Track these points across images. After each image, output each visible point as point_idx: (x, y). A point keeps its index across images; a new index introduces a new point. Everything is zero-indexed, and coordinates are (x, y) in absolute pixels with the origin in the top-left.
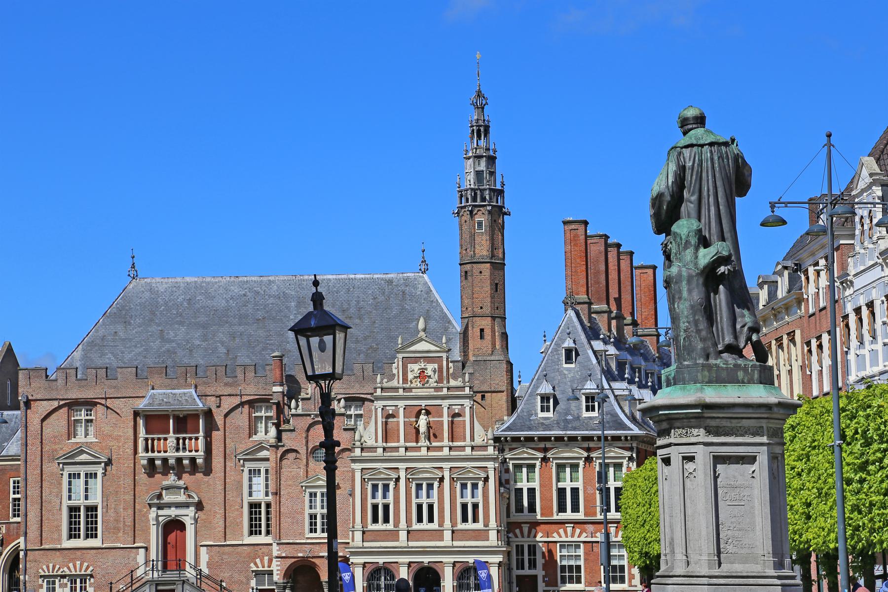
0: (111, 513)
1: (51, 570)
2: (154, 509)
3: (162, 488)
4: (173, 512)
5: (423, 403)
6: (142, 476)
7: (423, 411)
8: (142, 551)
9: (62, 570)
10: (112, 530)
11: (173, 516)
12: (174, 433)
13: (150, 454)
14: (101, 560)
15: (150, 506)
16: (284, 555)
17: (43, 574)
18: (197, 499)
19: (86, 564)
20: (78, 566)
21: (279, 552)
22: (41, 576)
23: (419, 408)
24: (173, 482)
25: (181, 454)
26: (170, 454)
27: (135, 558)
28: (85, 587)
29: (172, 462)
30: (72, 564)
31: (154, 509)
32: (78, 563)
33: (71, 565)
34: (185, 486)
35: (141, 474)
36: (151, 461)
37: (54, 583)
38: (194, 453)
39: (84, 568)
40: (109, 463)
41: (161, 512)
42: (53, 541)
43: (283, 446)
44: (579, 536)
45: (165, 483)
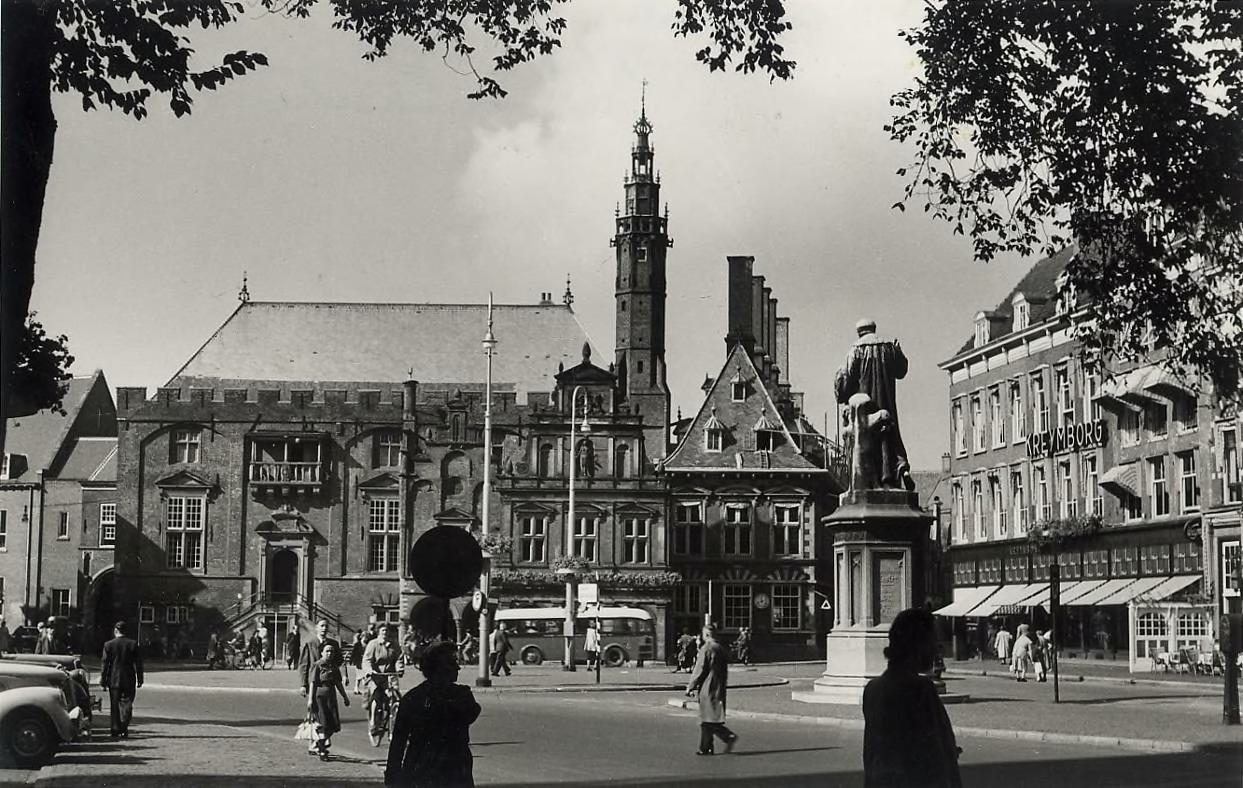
4: (285, 543)
12: (289, 460)
16: (412, 591)
41: (272, 543)
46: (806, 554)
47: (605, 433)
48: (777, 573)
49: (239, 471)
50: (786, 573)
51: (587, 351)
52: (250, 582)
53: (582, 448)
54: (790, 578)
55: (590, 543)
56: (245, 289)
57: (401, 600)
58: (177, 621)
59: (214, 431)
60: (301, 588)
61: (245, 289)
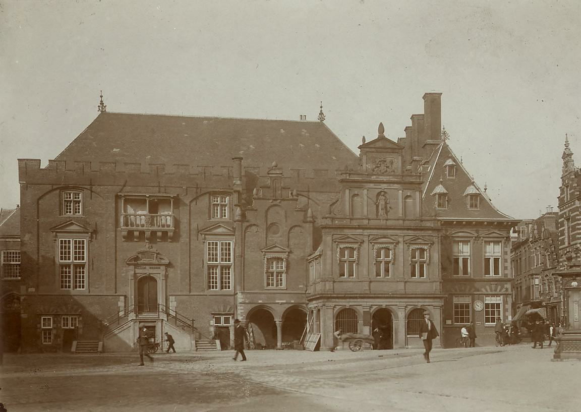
4: (148, 271)
5: (384, 186)
7: (383, 193)
8: (122, 298)
13: (130, 227)
16: (247, 302)
18: (167, 262)
21: (243, 300)
23: (380, 190)
24: (148, 249)
25: (155, 228)
26: (147, 228)
29: (148, 234)
31: (132, 267)
34: (157, 252)
36: (131, 233)
38: (166, 228)
40: (95, 232)
41: (138, 271)
43: (248, 221)
44: (469, 291)
45: (142, 250)
46: (506, 275)
47: (396, 186)
48: (488, 287)
49: (112, 221)
50: (493, 286)
51: (381, 128)
52: (123, 297)
53: (381, 197)
54: (496, 291)
55: (387, 263)
56: (102, 103)
57: (238, 308)
58: (70, 327)
59: (92, 191)
60: (161, 300)
61: (102, 103)
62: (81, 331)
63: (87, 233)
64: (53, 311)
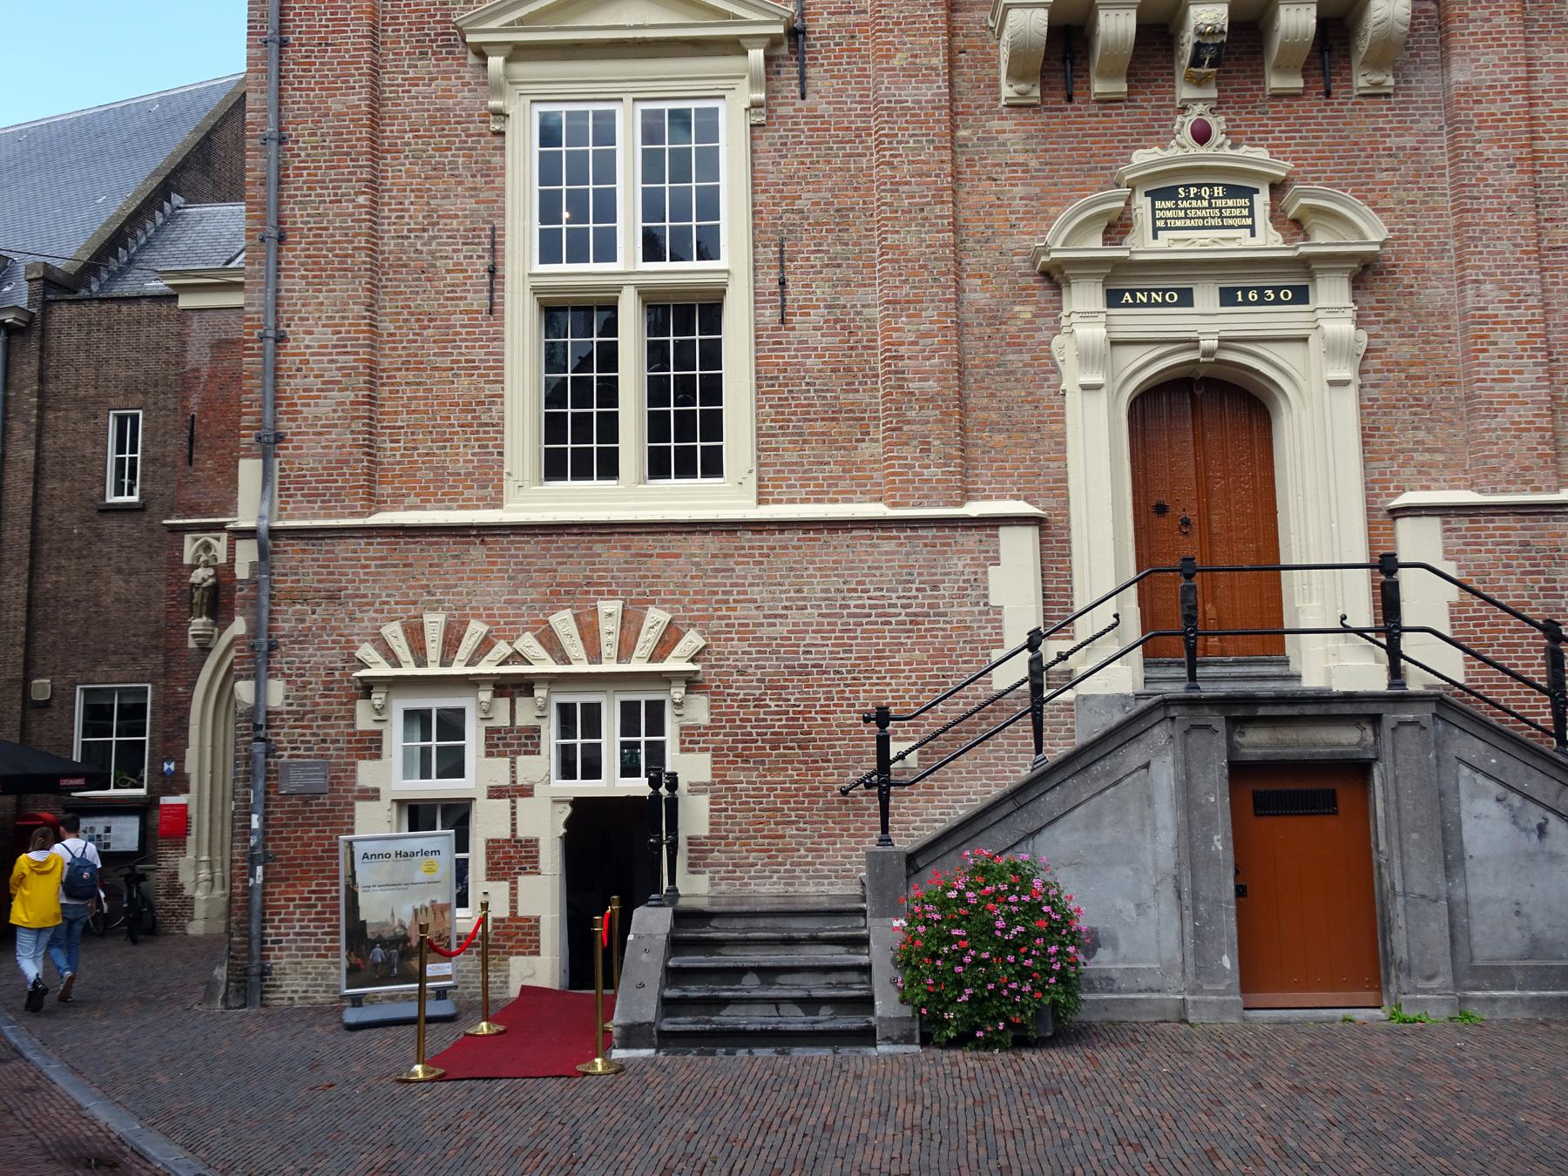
0: (809, 328)
1: (434, 650)
2: (1085, 298)
3: (1132, 186)
6: (995, 124)
8: (1020, 547)
9: (502, 649)
10: (819, 426)
11: (1209, 343)
14: (756, 593)
15: (1055, 277)
17: (383, 669)
19: (657, 618)
20: (609, 629)
22: (367, 687)
27: (979, 583)
28: (656, 752)
30: (567, 614)
31: (1085, 298)
32: (610, 608)
33: (563, 623)
35: (992, 111)
37: (452, 724)
39: (648, 638)
41: (1133, 322)
42: (439, 490)
52: (1029, 535)
62: (695, 817)
63: (735, 47)
64: (486, 645)
